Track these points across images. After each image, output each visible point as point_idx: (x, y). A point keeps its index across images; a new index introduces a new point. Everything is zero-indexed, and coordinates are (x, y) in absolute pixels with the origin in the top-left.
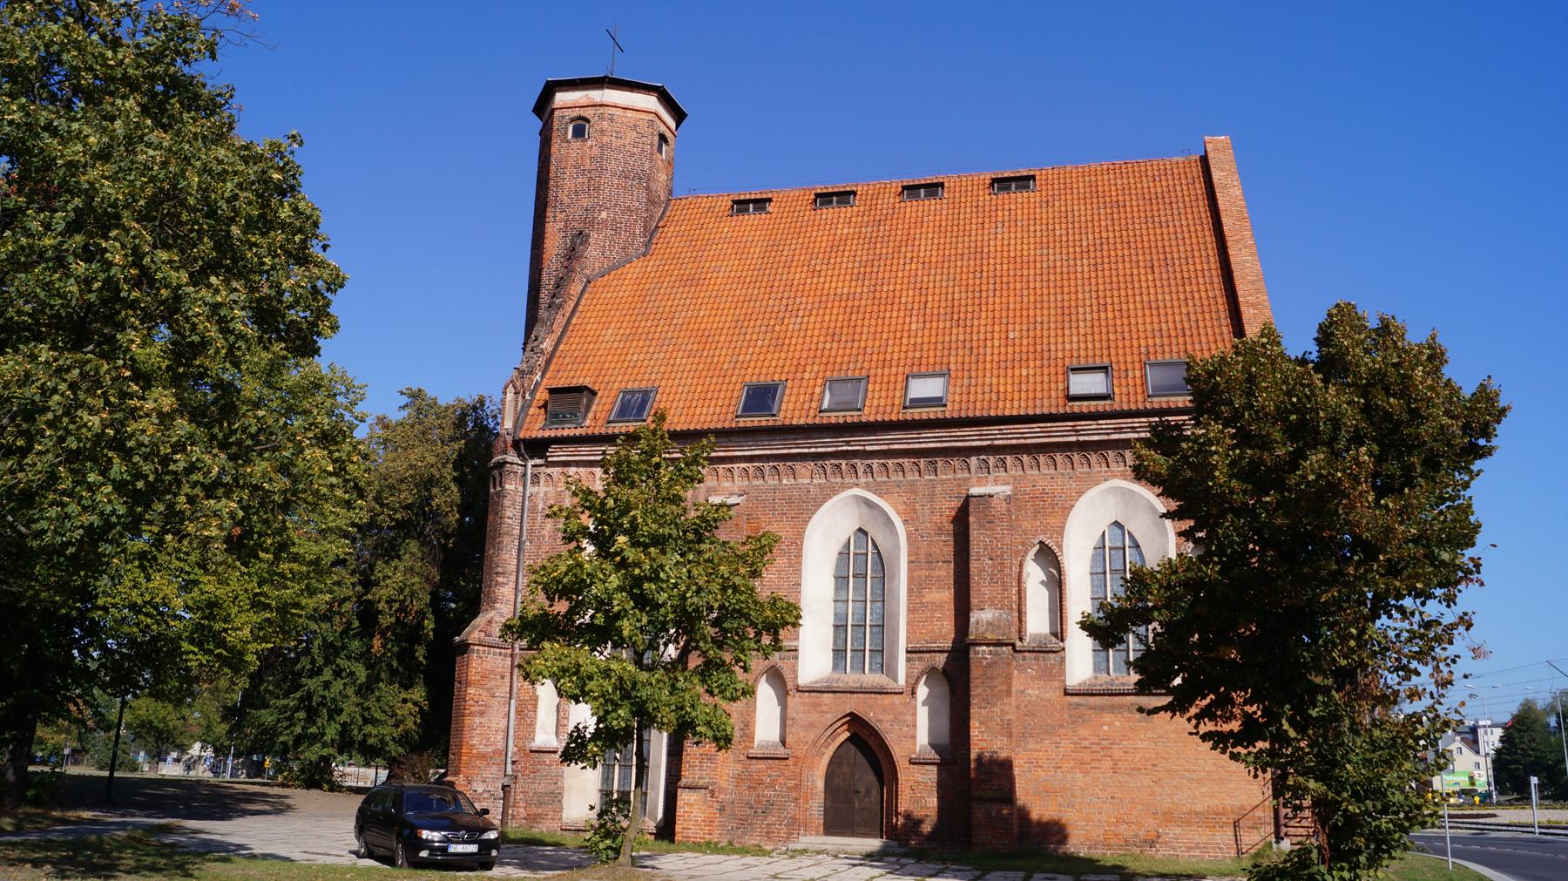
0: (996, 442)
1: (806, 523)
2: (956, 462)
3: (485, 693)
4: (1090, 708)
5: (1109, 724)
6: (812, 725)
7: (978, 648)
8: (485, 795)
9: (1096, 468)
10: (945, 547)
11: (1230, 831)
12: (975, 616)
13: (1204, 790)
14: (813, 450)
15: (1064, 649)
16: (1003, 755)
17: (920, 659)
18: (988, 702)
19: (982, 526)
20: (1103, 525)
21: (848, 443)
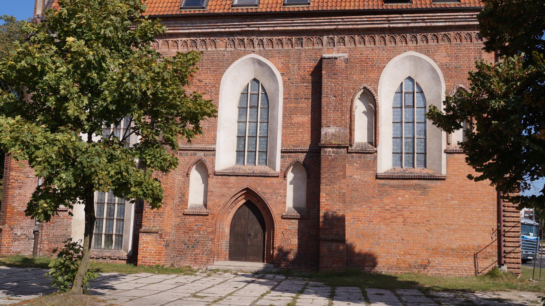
0: (340, 27)
1: (222, 74)
2: (314, 39)
3: (22, 175)
4: (392, 186)
5: (402, 197)
6: (223, 196)
7: (326, 149)
8: (23, 237)
9: (399, 44)
10: (306, 90)
11: (471, 260)
12: (324, 131)
13: (457, 236)
14: (227, 30)
15: (376, 152)
16: (340, 213)
17: (289, 157)
18: (331, 182)
19: (329, 77)
20: (402, 78)
21: (248, 26)
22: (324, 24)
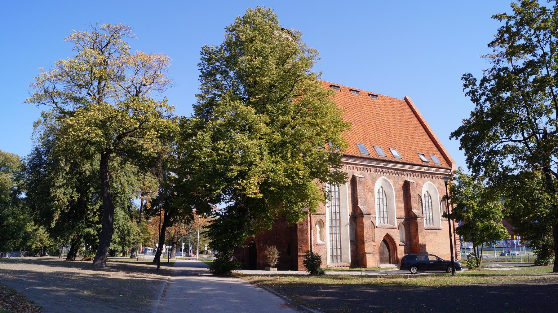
0: (411, 169)
1: (374, 184)
6: (380, 236)
10: (401, 193)
14: (376, 165)
16: (424, 243)
17: (399, 220)
19: (412, 190)
22: (407, 167)
